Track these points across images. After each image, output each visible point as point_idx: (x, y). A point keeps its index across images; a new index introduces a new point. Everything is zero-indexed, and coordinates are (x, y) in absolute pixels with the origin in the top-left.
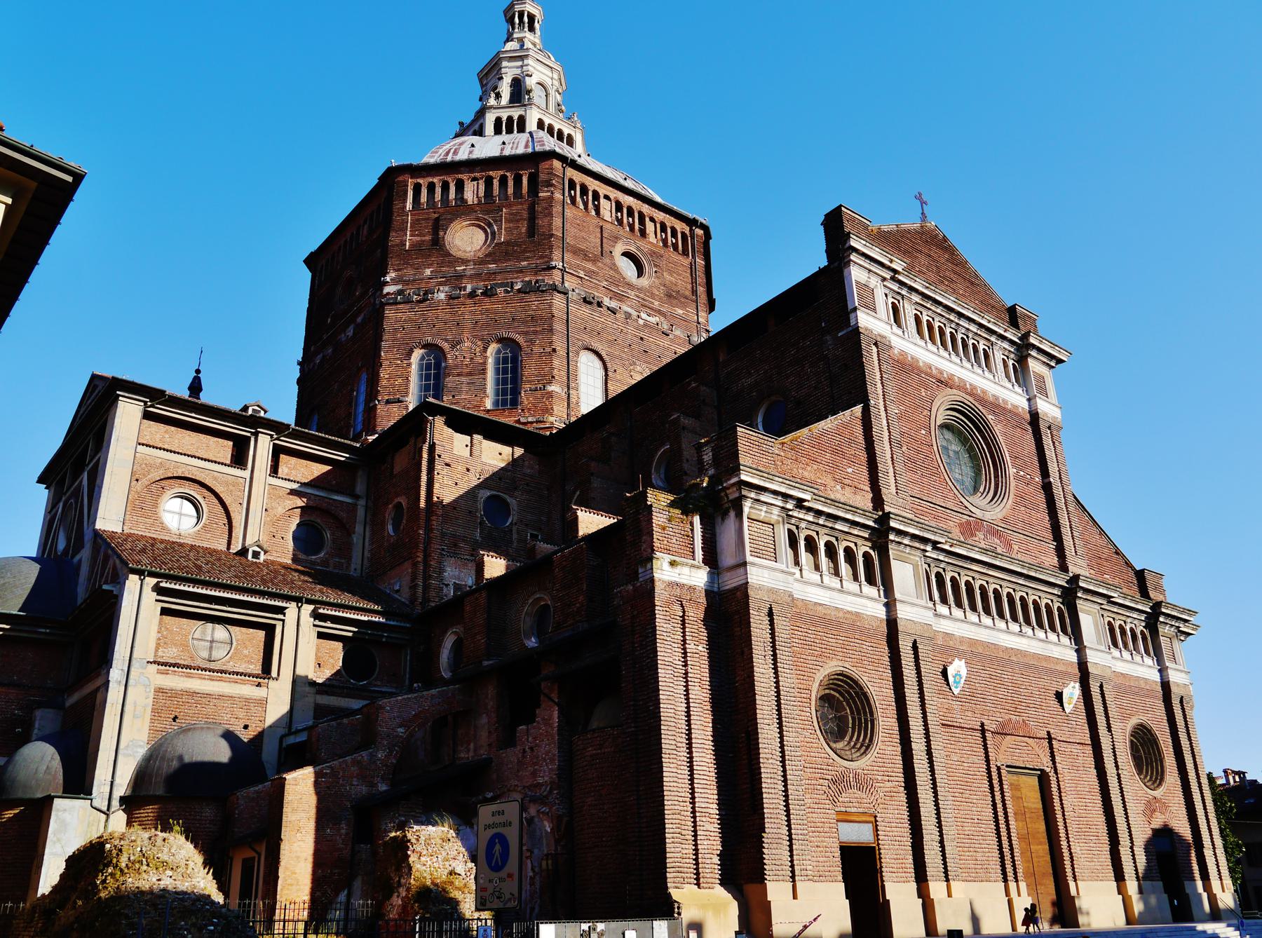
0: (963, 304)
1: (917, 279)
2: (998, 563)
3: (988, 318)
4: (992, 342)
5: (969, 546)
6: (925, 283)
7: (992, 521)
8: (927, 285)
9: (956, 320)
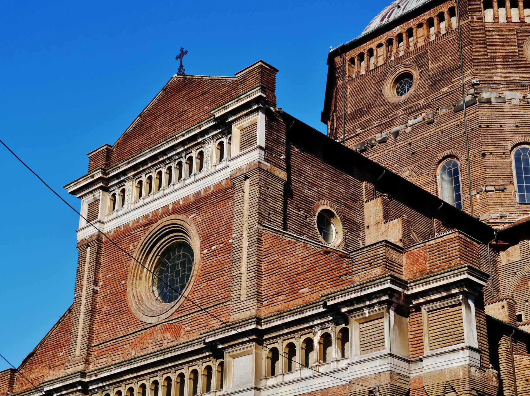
0: (157, 146)
1: (119, 165)
2: (135, 366)
3: (180, 134)
4: (201, 141)
5: (106, 369)
6: (125, 162)
7: (166, 320)
8: (127, 161)
9: (165, 157)
